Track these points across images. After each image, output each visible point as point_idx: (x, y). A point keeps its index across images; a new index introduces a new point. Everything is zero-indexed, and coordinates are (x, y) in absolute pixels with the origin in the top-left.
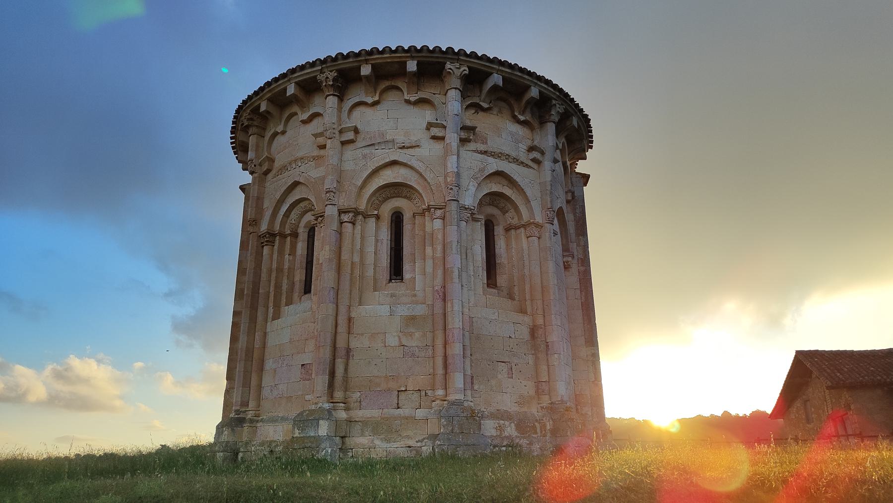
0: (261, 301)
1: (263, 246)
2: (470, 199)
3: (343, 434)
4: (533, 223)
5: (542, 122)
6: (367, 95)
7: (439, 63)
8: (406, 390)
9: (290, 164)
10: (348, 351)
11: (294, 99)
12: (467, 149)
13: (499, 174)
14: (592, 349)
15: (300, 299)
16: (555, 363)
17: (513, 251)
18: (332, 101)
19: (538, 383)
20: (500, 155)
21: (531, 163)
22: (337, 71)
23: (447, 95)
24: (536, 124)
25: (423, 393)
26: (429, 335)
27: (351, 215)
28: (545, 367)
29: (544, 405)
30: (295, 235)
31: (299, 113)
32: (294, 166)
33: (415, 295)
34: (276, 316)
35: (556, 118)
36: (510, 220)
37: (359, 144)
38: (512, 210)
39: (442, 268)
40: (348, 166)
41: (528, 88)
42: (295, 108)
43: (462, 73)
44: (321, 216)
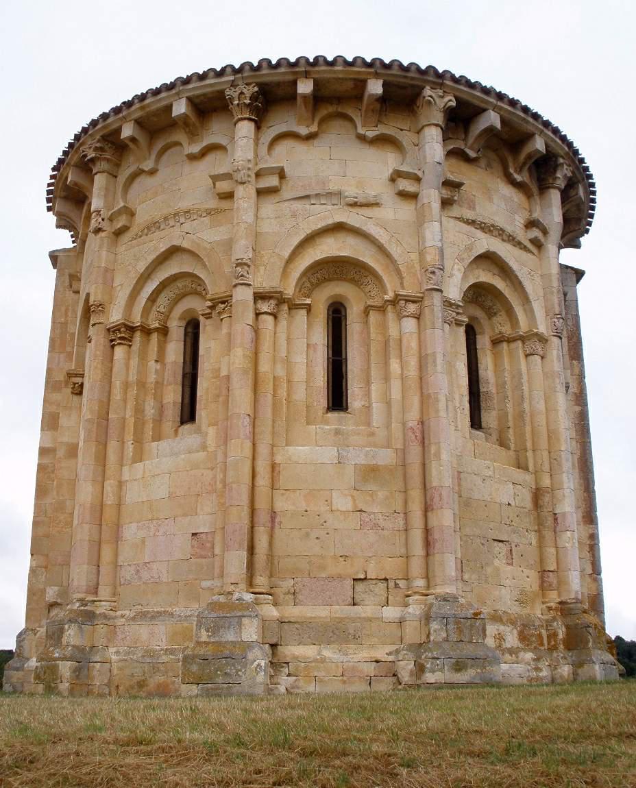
0: (113, 432)
1: (113, 347)
2: (454, 291)
3: (273, 641)
4: (537, 334)
5: (543, 188)
6: (299, 123)
7: (413, 86)
8: (365, 579)
9: (166, 219)
10: (273, 514)
11: (183, 122)
12: (448, 215)
13: (488, 258)
14: (589, 528)
15: (176, 431)
16: (567, 545)
17: (506, 375)
18: (245, 129)
19: (543, 572)
20: (492, 228)
21: (529, 245)
22: (258, 84)
23: (422, 132)
24: (535, 189)
25: (391, 584)
26: (399, 498)
27: (273, 302)
28: (553, 550)
29: (553, 605)
30: (164, 331)
31: (185, 144)
32: (172, 223)
33: (372, 434)
34: (139, 457)
35: (561, 183)
36: (500, 328)
37: (286, 193)
38: (503, 313)
39: (418, 394)
40: (267, 227)
41: (529, 136)
42: (180, 136)
43: (446, 105)
44: (223, 303)
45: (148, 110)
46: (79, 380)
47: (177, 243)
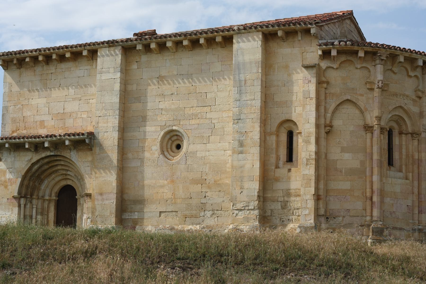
15: (390, 168)
32: (401, 97)
45: (411, 56)
46: (331, 128)
47: (403, 105)
